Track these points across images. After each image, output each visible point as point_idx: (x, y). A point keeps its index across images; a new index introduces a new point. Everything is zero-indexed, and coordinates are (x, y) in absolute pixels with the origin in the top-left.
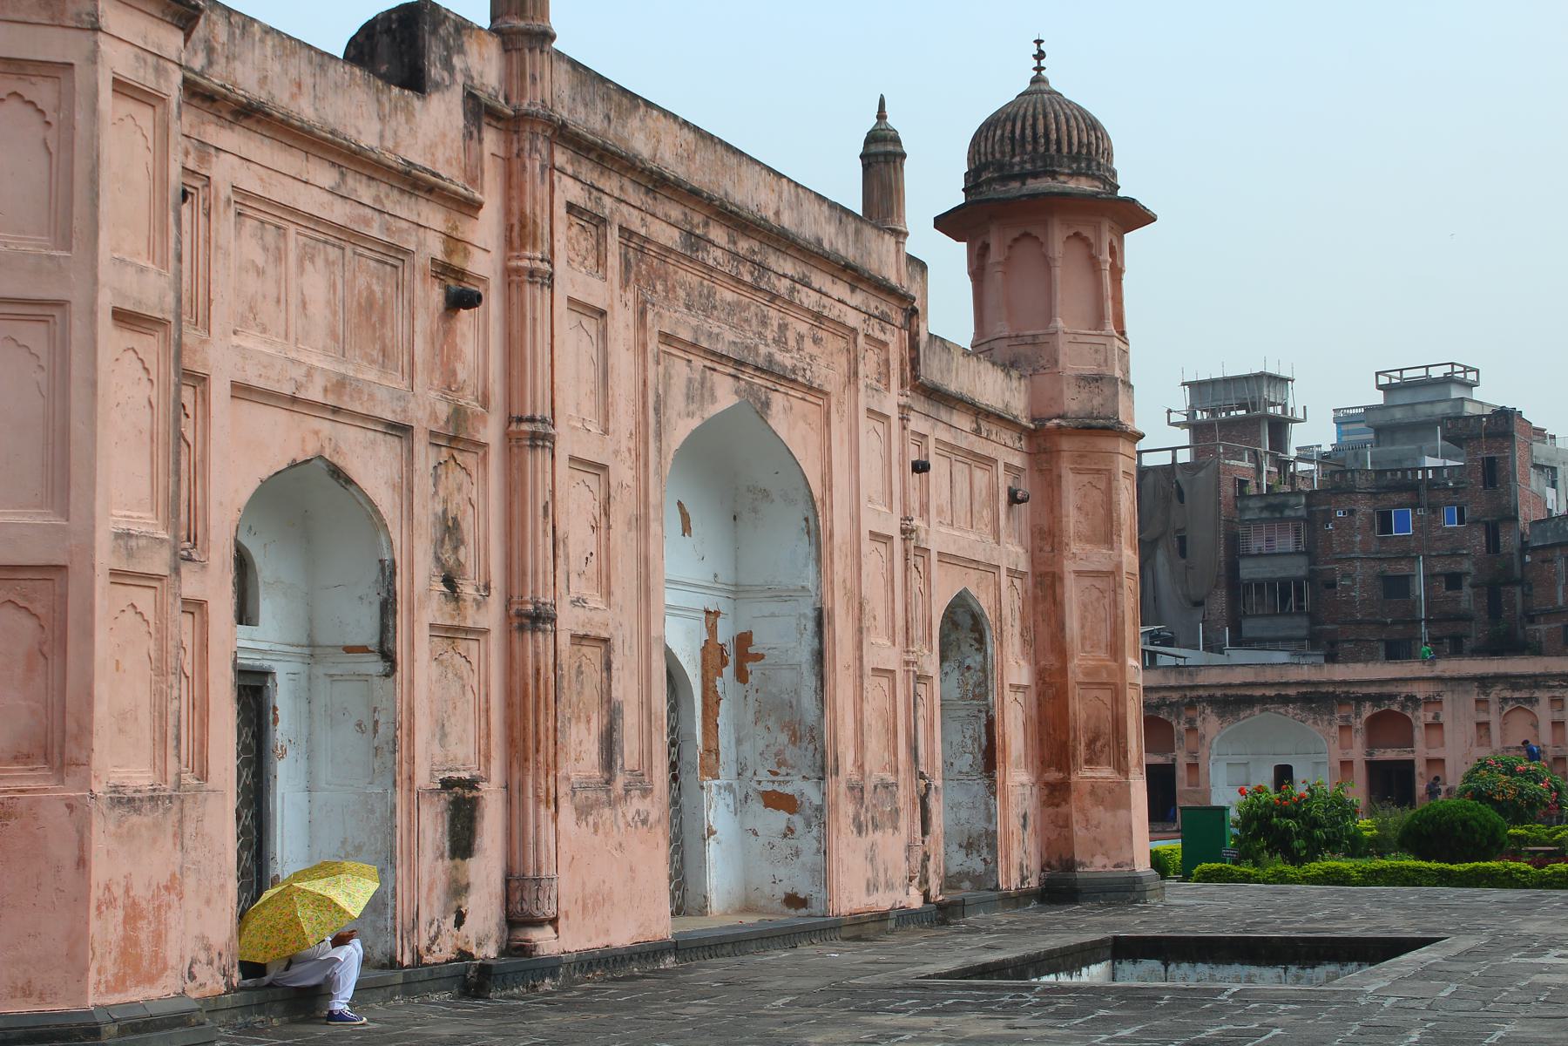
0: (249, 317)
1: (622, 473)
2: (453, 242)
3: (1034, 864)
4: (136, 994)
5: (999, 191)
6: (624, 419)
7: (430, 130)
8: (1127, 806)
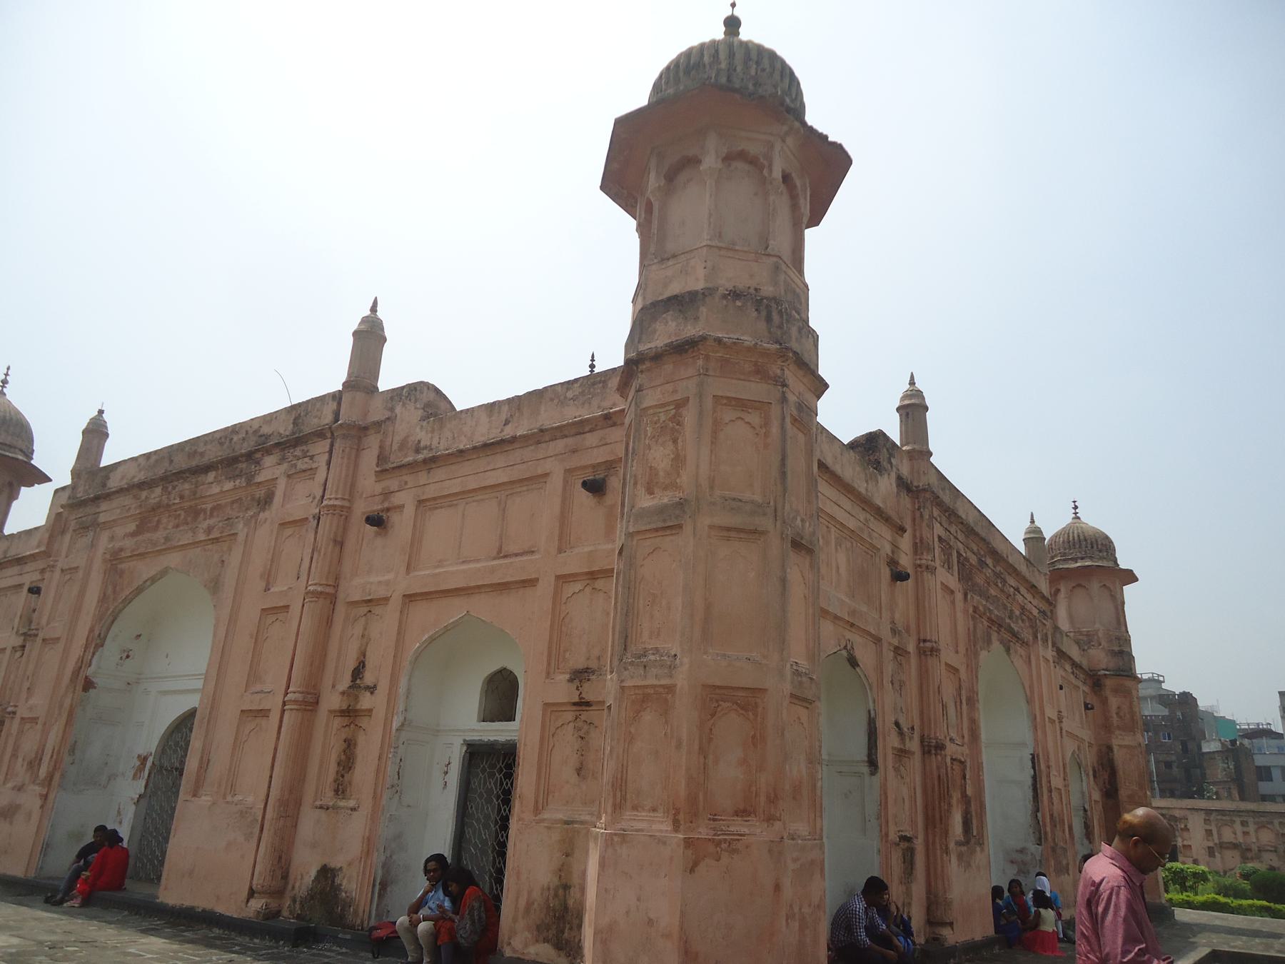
2: (895, 547)
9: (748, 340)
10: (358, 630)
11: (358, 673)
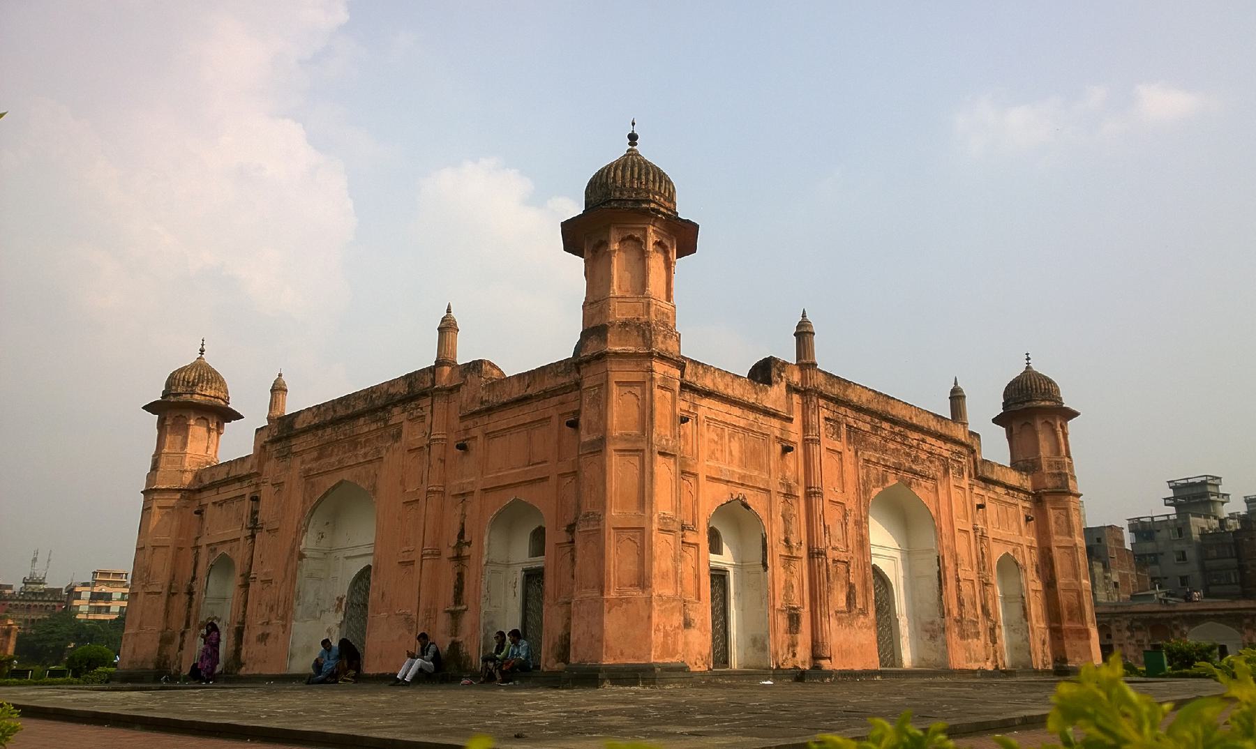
0: (712, 455)
1: (851, 505)
3: (1050, 660)
4: (668, 660)
5: (1013, 408)
6: (851, 489)
7: (775, 396)
8: (1088, 637)
9: (632, 349)
10: (459, 511)
11: (461, 535)
